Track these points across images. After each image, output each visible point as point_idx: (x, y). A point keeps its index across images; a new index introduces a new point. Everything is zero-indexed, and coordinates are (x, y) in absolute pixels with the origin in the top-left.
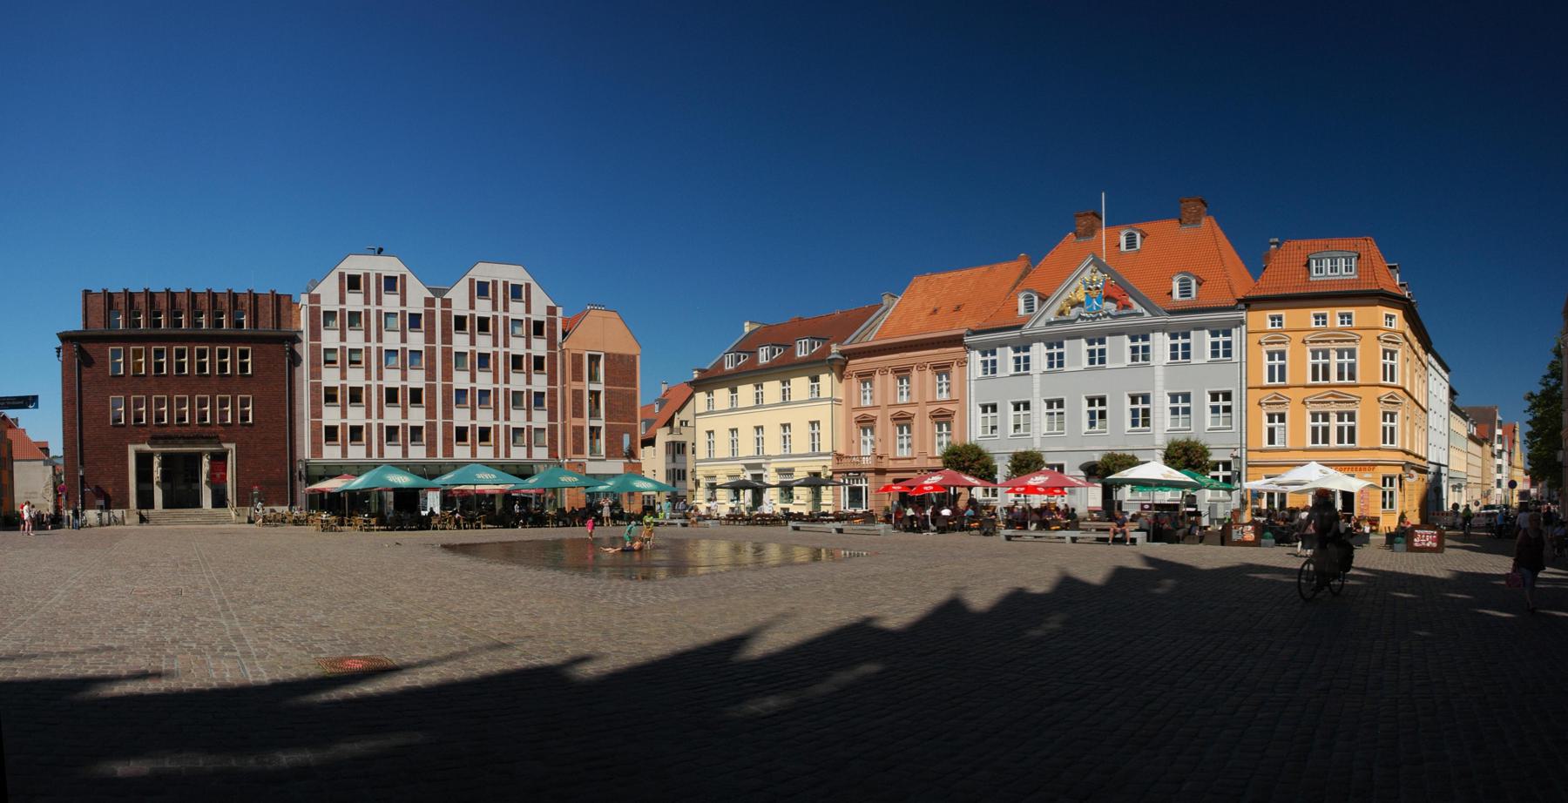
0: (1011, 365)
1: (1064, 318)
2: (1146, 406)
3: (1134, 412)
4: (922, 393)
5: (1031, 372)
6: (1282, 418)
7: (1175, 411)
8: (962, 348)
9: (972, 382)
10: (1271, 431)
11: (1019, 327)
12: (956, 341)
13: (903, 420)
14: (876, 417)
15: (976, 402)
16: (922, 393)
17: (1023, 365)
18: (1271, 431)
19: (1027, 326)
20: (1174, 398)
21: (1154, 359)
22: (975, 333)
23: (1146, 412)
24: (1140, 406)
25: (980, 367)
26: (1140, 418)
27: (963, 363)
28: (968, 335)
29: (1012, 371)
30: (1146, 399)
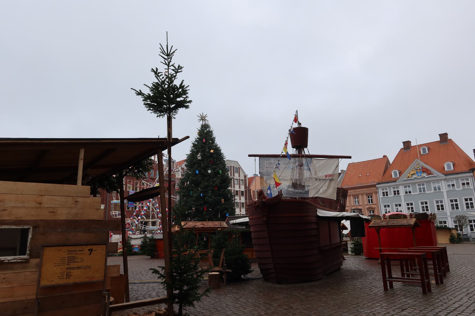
0: (393, 193)
1: (409, 179)
3: (438, 206)
4: (363, 202)
5: (400, 195)
8: (375, 188)
9: (380, 199)
11: (395, 181)
12: (374, 186)
14: (348, 210)
15: (382, 204)
16: (363, 202)
17: (397, 193)
19: (398, 181)
21: (443, 190)
22: (379, 184)
23: (442, 206)
25: (382, 194)
27: (376, 193)
28: (377, 185)
29: (393, 195)
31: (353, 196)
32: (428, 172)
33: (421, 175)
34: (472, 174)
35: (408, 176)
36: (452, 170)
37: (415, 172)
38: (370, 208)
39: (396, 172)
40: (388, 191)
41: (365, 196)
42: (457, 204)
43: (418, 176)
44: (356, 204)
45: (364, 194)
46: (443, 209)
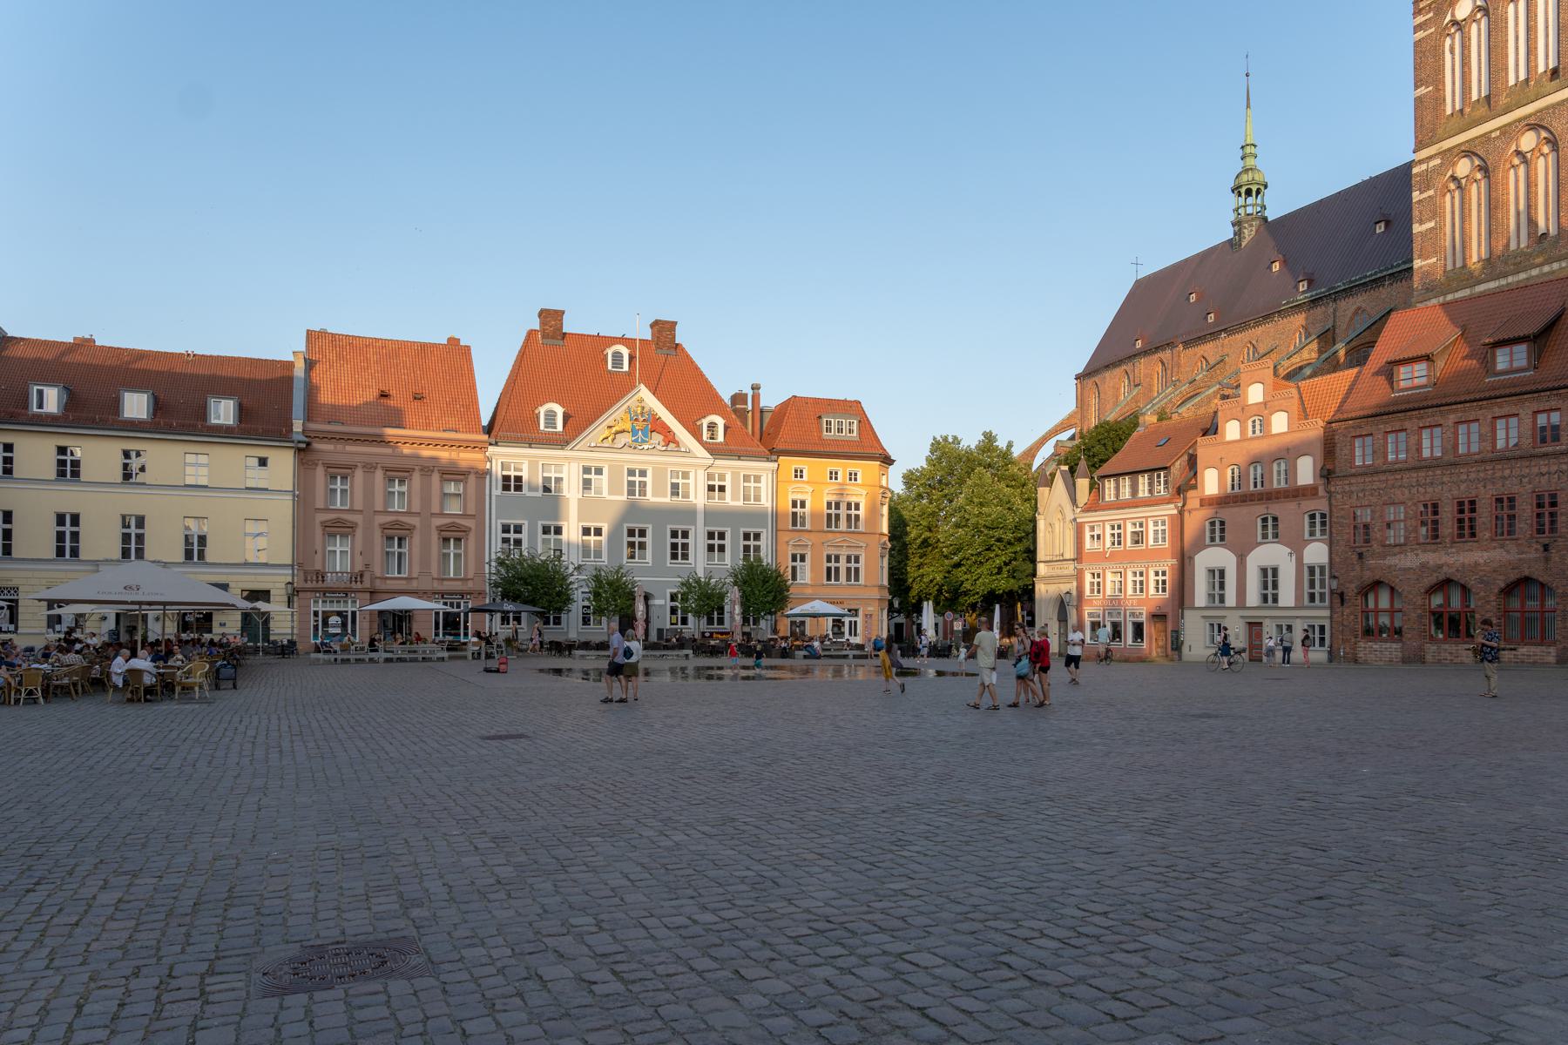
2: (711, 542)
3: (674, 546)
6: (803, 559)
7: (711, 548)
9: (493, 498)
10: (794, 569)
13: (397, 533)
15: (497, 519)
18: (794, 569)
20: (711, 535)
24: (680, 541)
26: (680, 551)
30: (685, 534)
31: (386, 470)
32: (670, 438)
33: (643, 441)
34: (776, 465)
35: (604, 436)
36: (719, 444)
37: (628, 426)
38: (397, 526)
39: (552, 411)
40: (564, 475)
41: (379, 474)
42: (688, 544)
43: (636, 441)
44: (335, 504)
45: (433, 471)
46: (685, 556)
